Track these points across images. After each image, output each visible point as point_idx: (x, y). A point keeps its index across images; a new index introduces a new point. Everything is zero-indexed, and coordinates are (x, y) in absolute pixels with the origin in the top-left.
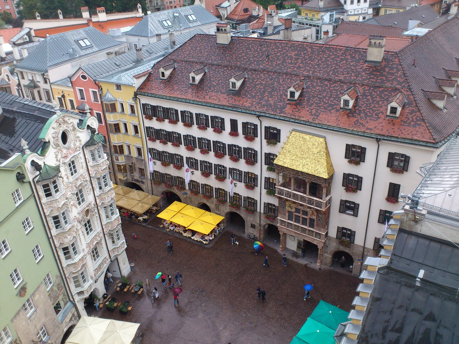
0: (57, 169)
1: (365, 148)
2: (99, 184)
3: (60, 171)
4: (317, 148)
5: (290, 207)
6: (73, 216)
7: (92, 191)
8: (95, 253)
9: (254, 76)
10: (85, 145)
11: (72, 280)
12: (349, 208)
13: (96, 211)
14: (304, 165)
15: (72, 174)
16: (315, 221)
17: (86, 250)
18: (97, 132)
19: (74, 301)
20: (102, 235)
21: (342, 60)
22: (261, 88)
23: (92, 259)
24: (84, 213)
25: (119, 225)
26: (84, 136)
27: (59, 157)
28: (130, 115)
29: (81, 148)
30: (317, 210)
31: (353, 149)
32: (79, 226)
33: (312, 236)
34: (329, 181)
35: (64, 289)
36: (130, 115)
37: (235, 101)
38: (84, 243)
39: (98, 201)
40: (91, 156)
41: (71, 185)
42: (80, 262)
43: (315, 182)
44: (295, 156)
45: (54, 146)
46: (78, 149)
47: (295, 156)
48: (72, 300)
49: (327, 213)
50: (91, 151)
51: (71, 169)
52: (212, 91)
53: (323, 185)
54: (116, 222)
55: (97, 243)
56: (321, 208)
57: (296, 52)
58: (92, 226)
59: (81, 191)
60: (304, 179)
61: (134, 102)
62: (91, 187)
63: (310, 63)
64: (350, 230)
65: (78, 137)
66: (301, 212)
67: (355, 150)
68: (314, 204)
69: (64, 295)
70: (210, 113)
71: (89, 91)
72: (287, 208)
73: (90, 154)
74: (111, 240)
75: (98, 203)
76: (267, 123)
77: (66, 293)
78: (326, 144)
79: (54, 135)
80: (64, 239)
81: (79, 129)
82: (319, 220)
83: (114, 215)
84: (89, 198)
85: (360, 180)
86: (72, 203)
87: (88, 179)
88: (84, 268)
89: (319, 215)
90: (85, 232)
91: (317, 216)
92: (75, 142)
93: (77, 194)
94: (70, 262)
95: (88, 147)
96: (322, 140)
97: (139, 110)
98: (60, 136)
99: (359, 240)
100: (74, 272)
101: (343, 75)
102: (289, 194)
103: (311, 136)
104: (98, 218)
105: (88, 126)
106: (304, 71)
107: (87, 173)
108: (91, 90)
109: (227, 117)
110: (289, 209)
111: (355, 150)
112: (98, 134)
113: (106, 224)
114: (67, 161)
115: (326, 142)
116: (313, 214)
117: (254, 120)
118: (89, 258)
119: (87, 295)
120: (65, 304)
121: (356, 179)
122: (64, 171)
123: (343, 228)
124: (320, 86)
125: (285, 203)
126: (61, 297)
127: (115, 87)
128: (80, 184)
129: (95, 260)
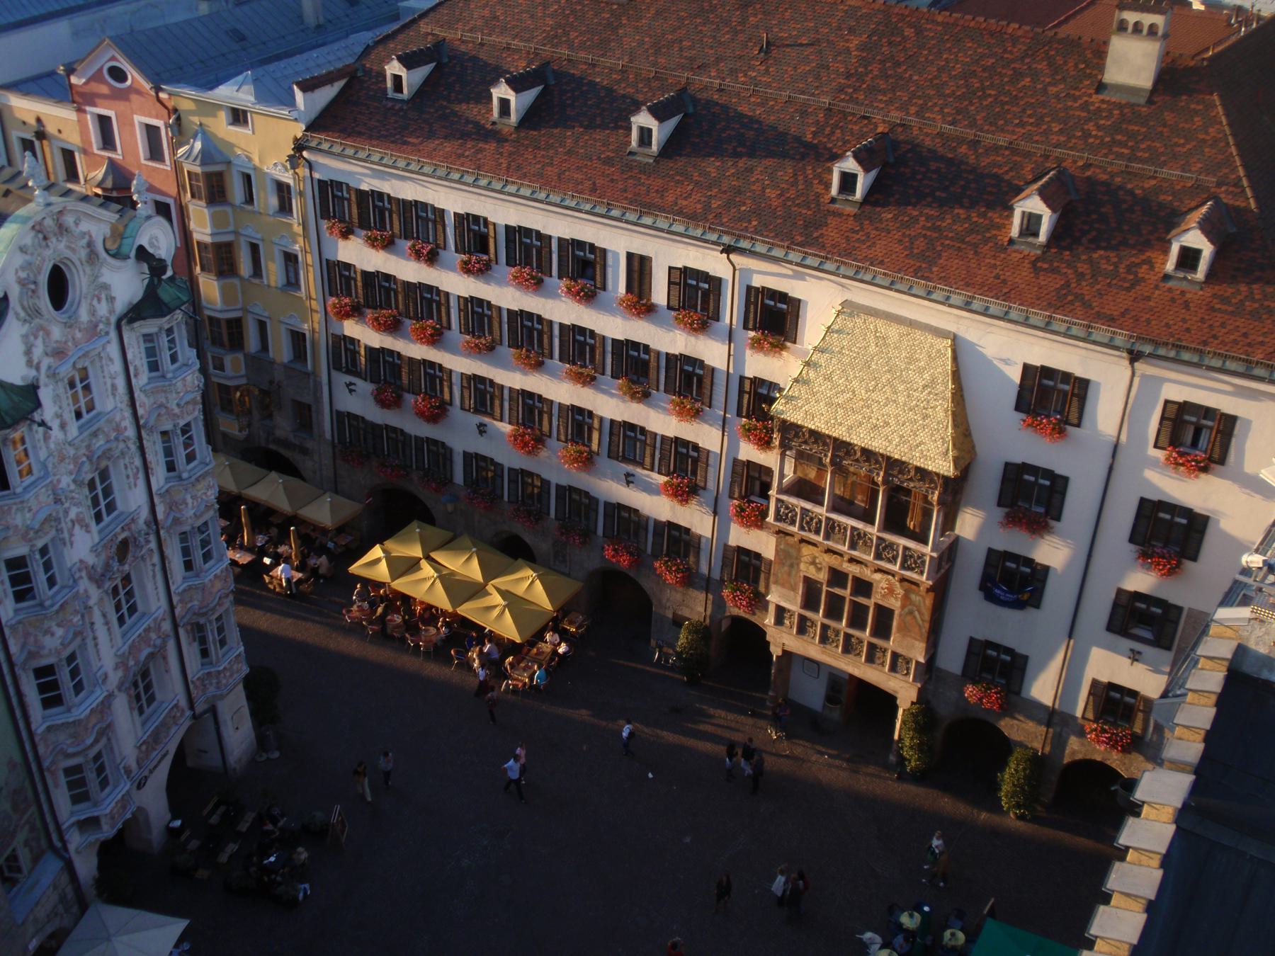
0: (30, 392)
2: (168, 452)
3: (38, 405)
5: (813, 563)
6: (76, 559)
7: (141, 475)
8: (141, 687)
10: (125, 315)
11: (63, 780)
13: (153, 545)
15: (78, 415)
17: (115, 678)
18: (169, 273)
19: (66, 849)
20: (167, 626)
21: (1018, 75)
23: (131, 709)
24: (114, 549)
25: (227, 596)
26: (126, 284)
27: (38, 351)
29: (113, 326)
31: (1046, 382)
32: (95, 593)
35: (33, 809)
38: (107, 652)
40: (144, 355)
41: (72, 452)
42: (93, 720)
45: (22, 314)
46: (101, 326)
48: (58, 844)
50: (148, 338)
51: (75, 399)
54: (218, 585)
55: (151, 656)
58: (138, 598)
59: (104, 475)
62: (138, 462)
64: (1009, 651)
65: (106, 287)
67: (1051, 383)
69: (32, 829)
70: (559, 225)
71: (132, 125)
72: (802, 566)
73: (143, 346)
74: (196, 647)
75: (160, 516)
77: (38, 824)
79: (23, 275)
80: (40, 637)
81: (110, 260)
82: (911, 613)
83: (211, 563)
84: (132, 499)
86: (73, 514)
87: (131, 432)
88: (104, 741)
90: (114, 618)
91: (906, 597)
92: (95, 302)
93: (92, 485)
94: (58, 716)
95: (136, 325)
98: (43, 279)
100: (71, 750)
103: (903, 329)
104: (158, 568)
105: (141, 249)
107: (128, 413)
108: (138, 119)
109: (616, 240)
110: (812, 573)
111: (1051, 383)
112: (172, 279)
113: (185, 591)
114: (66, 370)
116: (891, 591)
117: (712, 262)
118: (121, 708)
119: (108, 831)
120: (36, 860)
121: (1047, 483)
122: (52, 403)
125: (799, 550)
126: (22, 836)
128: (104, 453)
129: (141, 712)
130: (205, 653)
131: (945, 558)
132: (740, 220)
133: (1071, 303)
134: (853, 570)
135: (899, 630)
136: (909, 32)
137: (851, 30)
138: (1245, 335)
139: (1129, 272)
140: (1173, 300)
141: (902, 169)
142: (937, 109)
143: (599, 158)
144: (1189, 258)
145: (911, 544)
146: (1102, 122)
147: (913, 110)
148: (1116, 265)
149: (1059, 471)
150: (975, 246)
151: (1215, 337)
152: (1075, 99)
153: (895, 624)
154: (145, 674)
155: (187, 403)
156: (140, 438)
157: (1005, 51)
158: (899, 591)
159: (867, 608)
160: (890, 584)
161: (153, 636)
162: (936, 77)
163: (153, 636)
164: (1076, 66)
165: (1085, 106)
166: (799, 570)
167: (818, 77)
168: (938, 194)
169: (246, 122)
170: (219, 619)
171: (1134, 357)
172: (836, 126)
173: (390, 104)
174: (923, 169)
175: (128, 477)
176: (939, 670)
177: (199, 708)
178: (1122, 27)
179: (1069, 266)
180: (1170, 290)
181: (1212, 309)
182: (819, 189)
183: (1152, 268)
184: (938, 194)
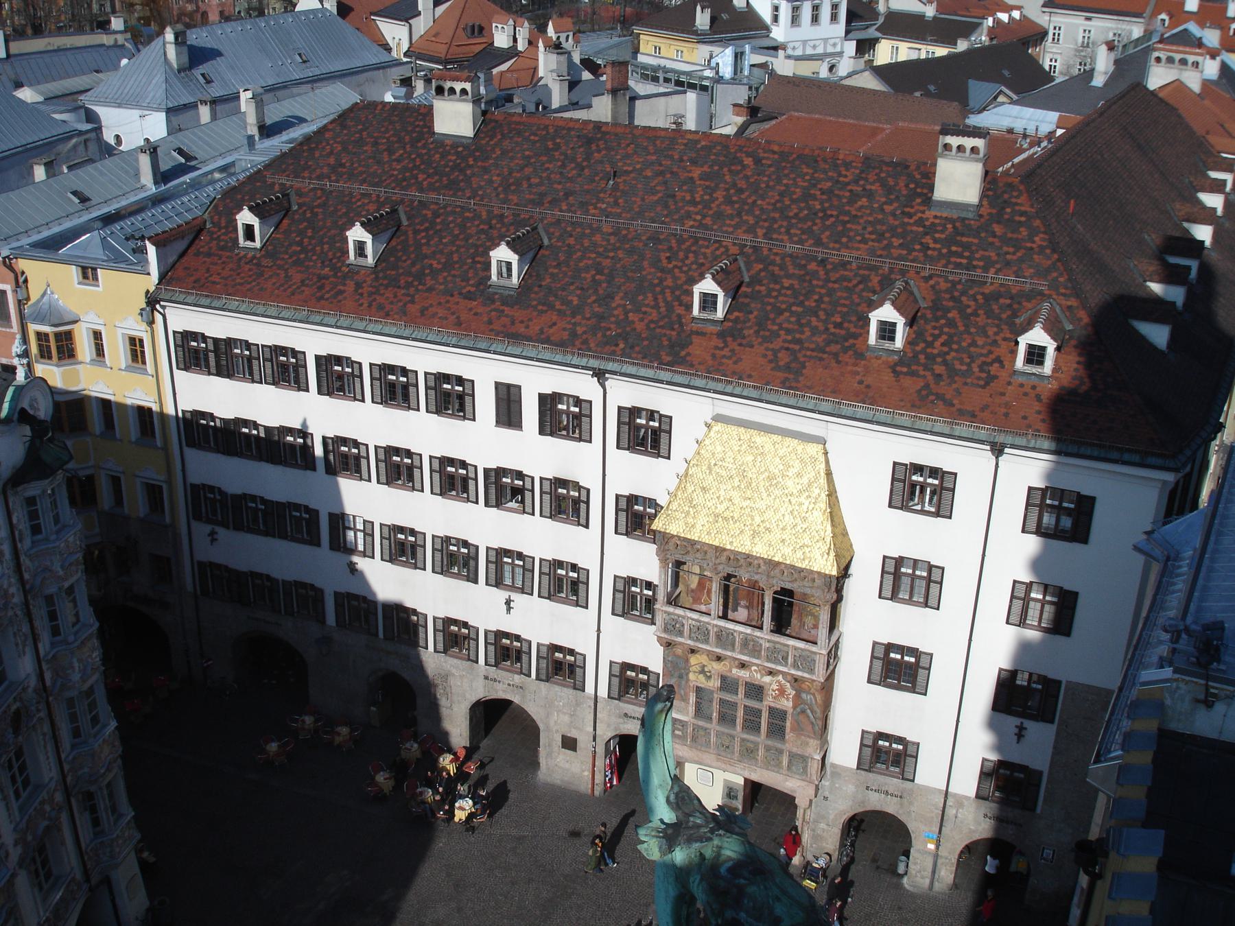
4: (799, 475)
5: (702, 672)
7: (30, 641)
12: (900, 669)
14: (755, 534)
16: (789, 717)
17: (15, 854)
20: (59, 797)
22: (599, 283)
28: (128, 369)
36: (128, 369)
37: (513, 323)
39: (48, 676)
44: (725, 505)
47: (725, 505)
52: (431, 289)
55: (48, 828)
57: (706, 169)
60: (756, 577)
61: (144, 326)
62: (26, 628)
64: (900, 740)
66: (741, 690)
68: (790, 660)
72: (692, 676)
75: (48, 683)
78: (827, 462)
82: (803, 712)
91: (797, 697)
96: (814, 449)
97: (161, 352)
99: (929, 772)
101: (864, 241)
103: (775, 437)
106: (736, 227)
109: (484, 371)
110: (701, 681)
113: (74, 758)
115: (826, 453)
116: (782, 691)
123: (881, 736)
125: (687, 660)
127: (74, 272)
129: (41, 888)
130: (96, 822)
132: (607, 343)
133: (932, 402)
134: (744, 674)
135: (792, 730)
136: (748, 161)
137: (694, 162)
139: (981, 371)
140: (1026, 394)
141: (757, 288)
142: (783, 230)
143: (460, 294)
145: (801, 645)
146: (937, 235)
147: (760, 232)
148: (969, 365)
150: (836, 355)
153: (788, 724)
154: (41, 850)
155: (71, 564)
156: (26, 604)
157: (840, 175)
158: (791, 692)
159: (760, 711)
161: (48, 808)
162: (778, 201)
163: (48, 808)
164: (907, 186)
166: (688, 680)
167: (666, 206)
168: (794, 308)
169: (96, 278)
170: (109, 785)
171: (998, 450)
172: (688, 250)
173: (243, 253)
174: (777, 287)
175: (17, 645)
176: (833, 765)
177: (94, 882)
178: (947, 147)
179: (926, 368)
180: (1022, 385)
182: (680, 310)
183: (1003, 366)
184: (794, 308)
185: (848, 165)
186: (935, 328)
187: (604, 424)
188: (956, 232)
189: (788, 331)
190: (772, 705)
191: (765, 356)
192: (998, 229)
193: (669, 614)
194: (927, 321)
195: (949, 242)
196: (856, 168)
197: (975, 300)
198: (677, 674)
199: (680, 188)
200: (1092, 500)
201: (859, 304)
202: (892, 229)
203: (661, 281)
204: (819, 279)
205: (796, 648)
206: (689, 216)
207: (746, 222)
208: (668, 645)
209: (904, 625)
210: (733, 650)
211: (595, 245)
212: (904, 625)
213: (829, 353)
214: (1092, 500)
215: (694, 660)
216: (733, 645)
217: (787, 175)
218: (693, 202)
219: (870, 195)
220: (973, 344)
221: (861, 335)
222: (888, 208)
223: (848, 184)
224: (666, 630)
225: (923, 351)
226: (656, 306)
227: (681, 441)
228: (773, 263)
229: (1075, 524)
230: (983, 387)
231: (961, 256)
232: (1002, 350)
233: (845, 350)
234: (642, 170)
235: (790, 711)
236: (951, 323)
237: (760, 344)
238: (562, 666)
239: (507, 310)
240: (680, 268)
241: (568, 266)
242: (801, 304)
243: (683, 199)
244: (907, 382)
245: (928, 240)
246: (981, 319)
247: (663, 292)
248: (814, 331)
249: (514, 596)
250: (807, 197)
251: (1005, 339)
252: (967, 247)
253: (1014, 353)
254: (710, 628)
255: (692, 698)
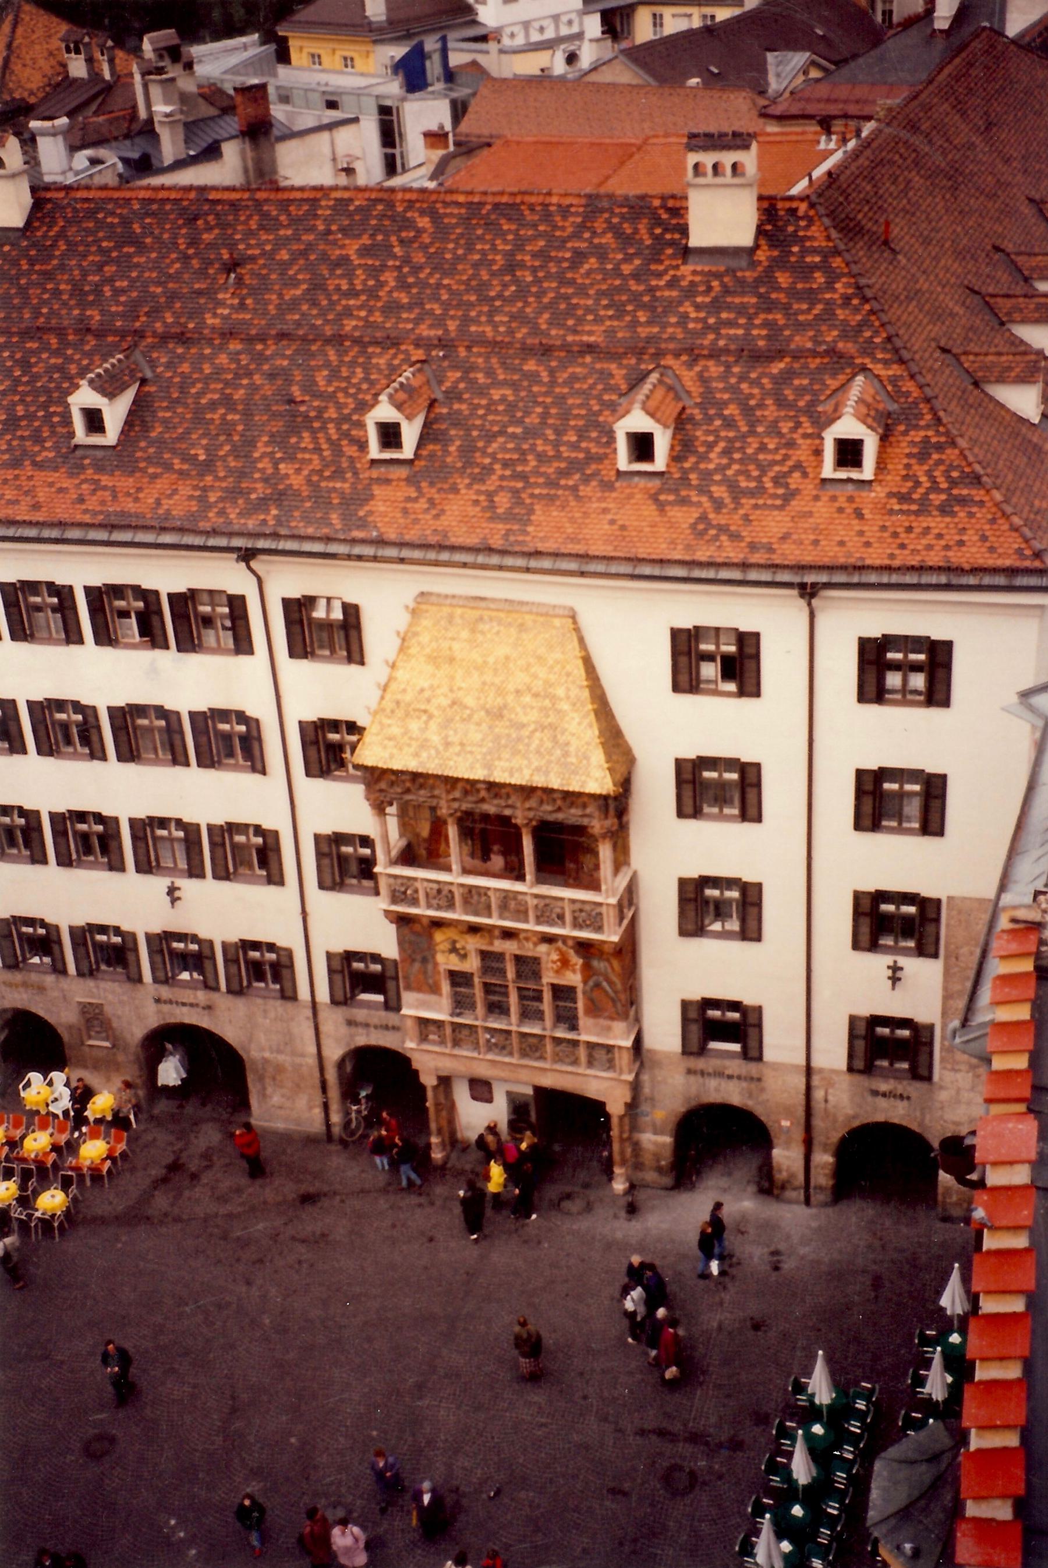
1: (757, 635)
5: (454, 950)
9: (185, 368)
21: (579, 257)
22: (234, 424)
30: (584, 947)
33: (575, 1062)
34: (617, 805)
43: (560, 816)
49: (628, 951)
53: (597, 825)
56: (599, 929)
57: (366, 240)
60: (507, 812)
63: (439, 286)
68: (568, 918)
72: (440, 958)
76: (288, 580)
82: (597, 985)
85: (751, 778)
89: (595, 963)
91: (587, 968)
99: (781, 1042)
101: (598, 320)
102: (443, 896)
106: (417, 321)
110: (454, 963)
116: (565, 963)
121: (735, 776)
123: (709, 1003)
124: (504, 383)
125: (431, 937)
131: (626, 903)
136: (424, 222)
138: (940, 536)
140: (840, 510)
141: (456, 406)
142: (483, 319)
144: (849, 453)
146: (699, 299)
148: (759, 479)
149: (745, 759)
150: (575, 489)
151: (902, 546)
152: (659, 275)
153: (580, 1005)
157: (555, 227)
158: (577, 961)
160: (562, 953)
162: (473, 277)
165: (673, 283)
167: (314, 303)
168: (510, 430)
171: (808, 592)
172: (353, 364)
174: (484, 402)
179: (703, 490)
181: (891, 512)
182: (351, 451)
183: (805, 475)
184: (510, 430)
185: (565, 211)
186: (708, 432)
187: (268, 626)
188: (726, 291)
189: (506, 464)
190: (555, 981)
191: (476, 502)
192: (783, 279)
193: (396, 877)
194: (696, 424)
195: (716, 306)
196: (577, 214)
197: (762, 387)
198: (419, 957)
199: (332, 271)
200: (948, 645)
201: (600, 413)
202: (635, 298)
203: (321, 411)
204: (540, 383)
205: (573, 901)
206: (348, 312)
207: (431, 312)
208: (402, 921)
209: (717, 847)
210: (490, 916)
211: (219, 371)
212: (717, 847)
213: (566, 488)
214: (948, 645)
215: (439, 936)
216: (489, 907)
217: (481, 238)
218: (353, 293)
219: (601, 253)
220: (763, 448)
221: (606, 456)
222: (626, 269)
223: (570, 238)
224: (394, 900)
225: (693, 469)
226: (318, 450)
227: (378, 635)
228: (473, 368)
229: (931, 682)
230: (781, 508)
231: (730, 324)
232: (802, 453)
233: (586, 480)
234: (274, 251)
235: (580, 987)
236: (729, 423)
237: (469, 486)
238: (260, 967)
239: (105, 480)
240: (345, 390)
241: (186, 405)
242: (520, 422)
243: (338, 288)
244: (676, 513)
245: (688, 308)
246: (771, 412)
247: (324, 428)
248: (541, 458)
249: (180, 882)
250: (511, 267)
251: (806, 436)
252: (741, 310)
253: (818, 452)
254: (454, 889)
255: (446, 987)
